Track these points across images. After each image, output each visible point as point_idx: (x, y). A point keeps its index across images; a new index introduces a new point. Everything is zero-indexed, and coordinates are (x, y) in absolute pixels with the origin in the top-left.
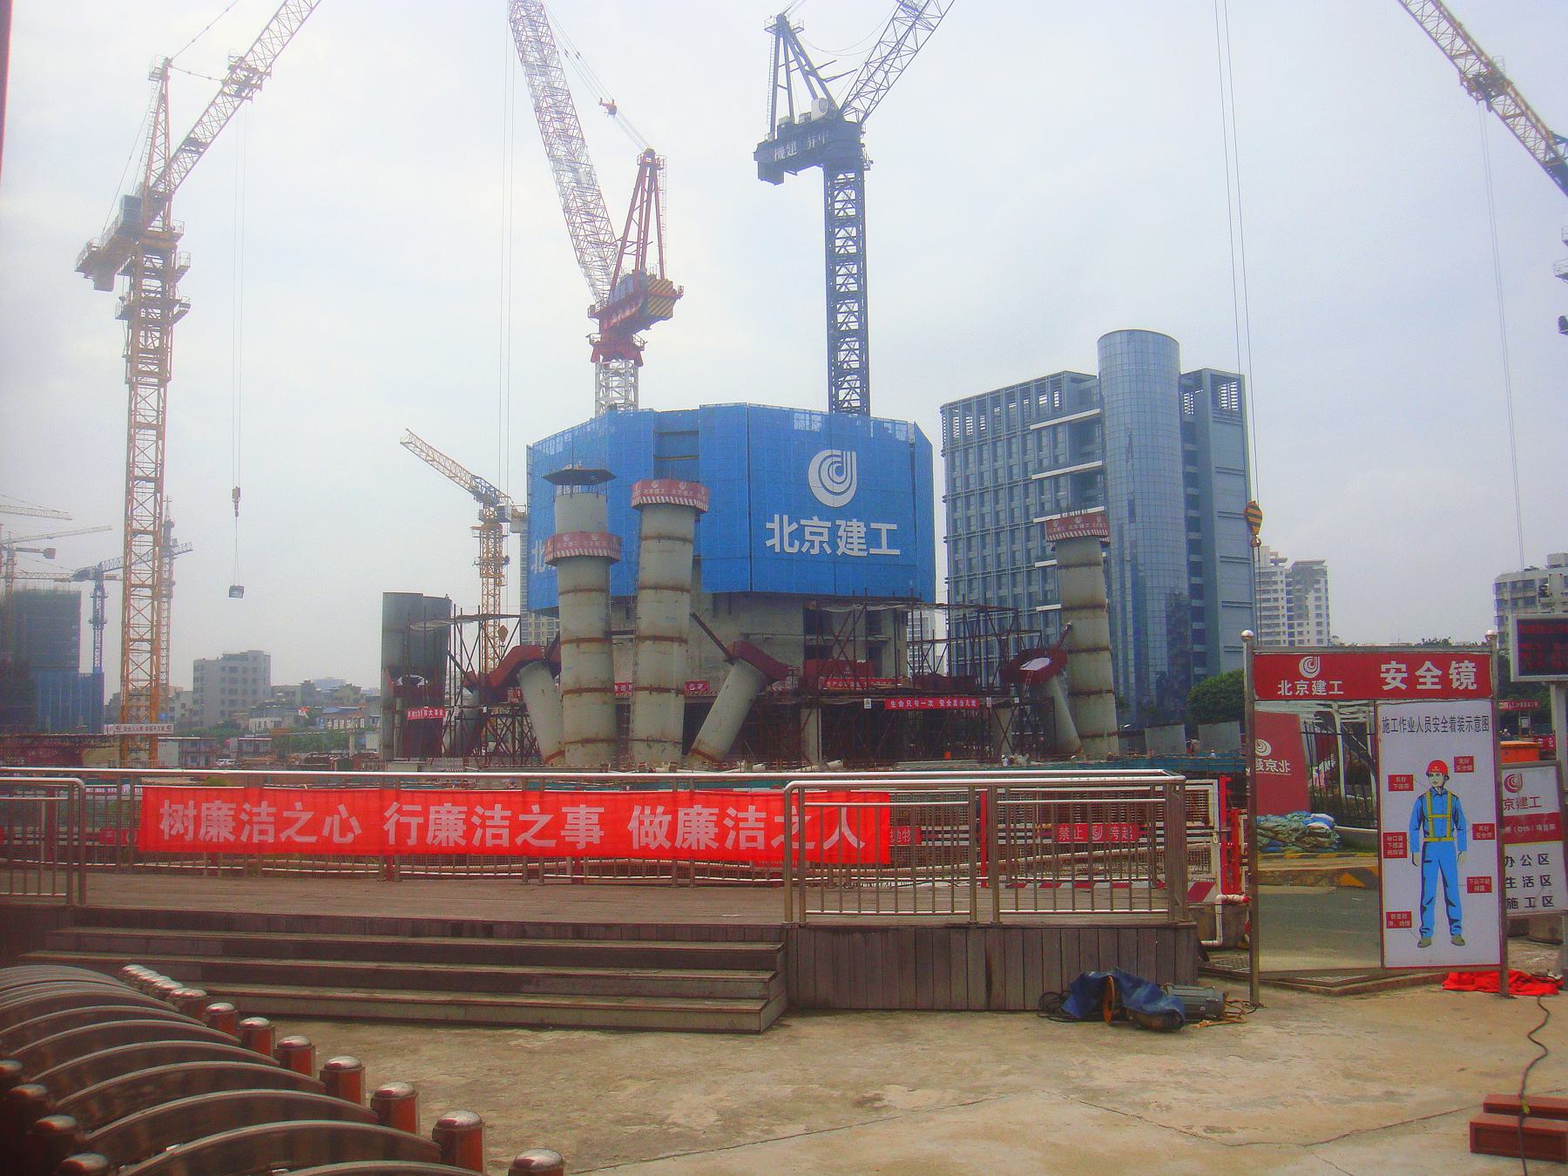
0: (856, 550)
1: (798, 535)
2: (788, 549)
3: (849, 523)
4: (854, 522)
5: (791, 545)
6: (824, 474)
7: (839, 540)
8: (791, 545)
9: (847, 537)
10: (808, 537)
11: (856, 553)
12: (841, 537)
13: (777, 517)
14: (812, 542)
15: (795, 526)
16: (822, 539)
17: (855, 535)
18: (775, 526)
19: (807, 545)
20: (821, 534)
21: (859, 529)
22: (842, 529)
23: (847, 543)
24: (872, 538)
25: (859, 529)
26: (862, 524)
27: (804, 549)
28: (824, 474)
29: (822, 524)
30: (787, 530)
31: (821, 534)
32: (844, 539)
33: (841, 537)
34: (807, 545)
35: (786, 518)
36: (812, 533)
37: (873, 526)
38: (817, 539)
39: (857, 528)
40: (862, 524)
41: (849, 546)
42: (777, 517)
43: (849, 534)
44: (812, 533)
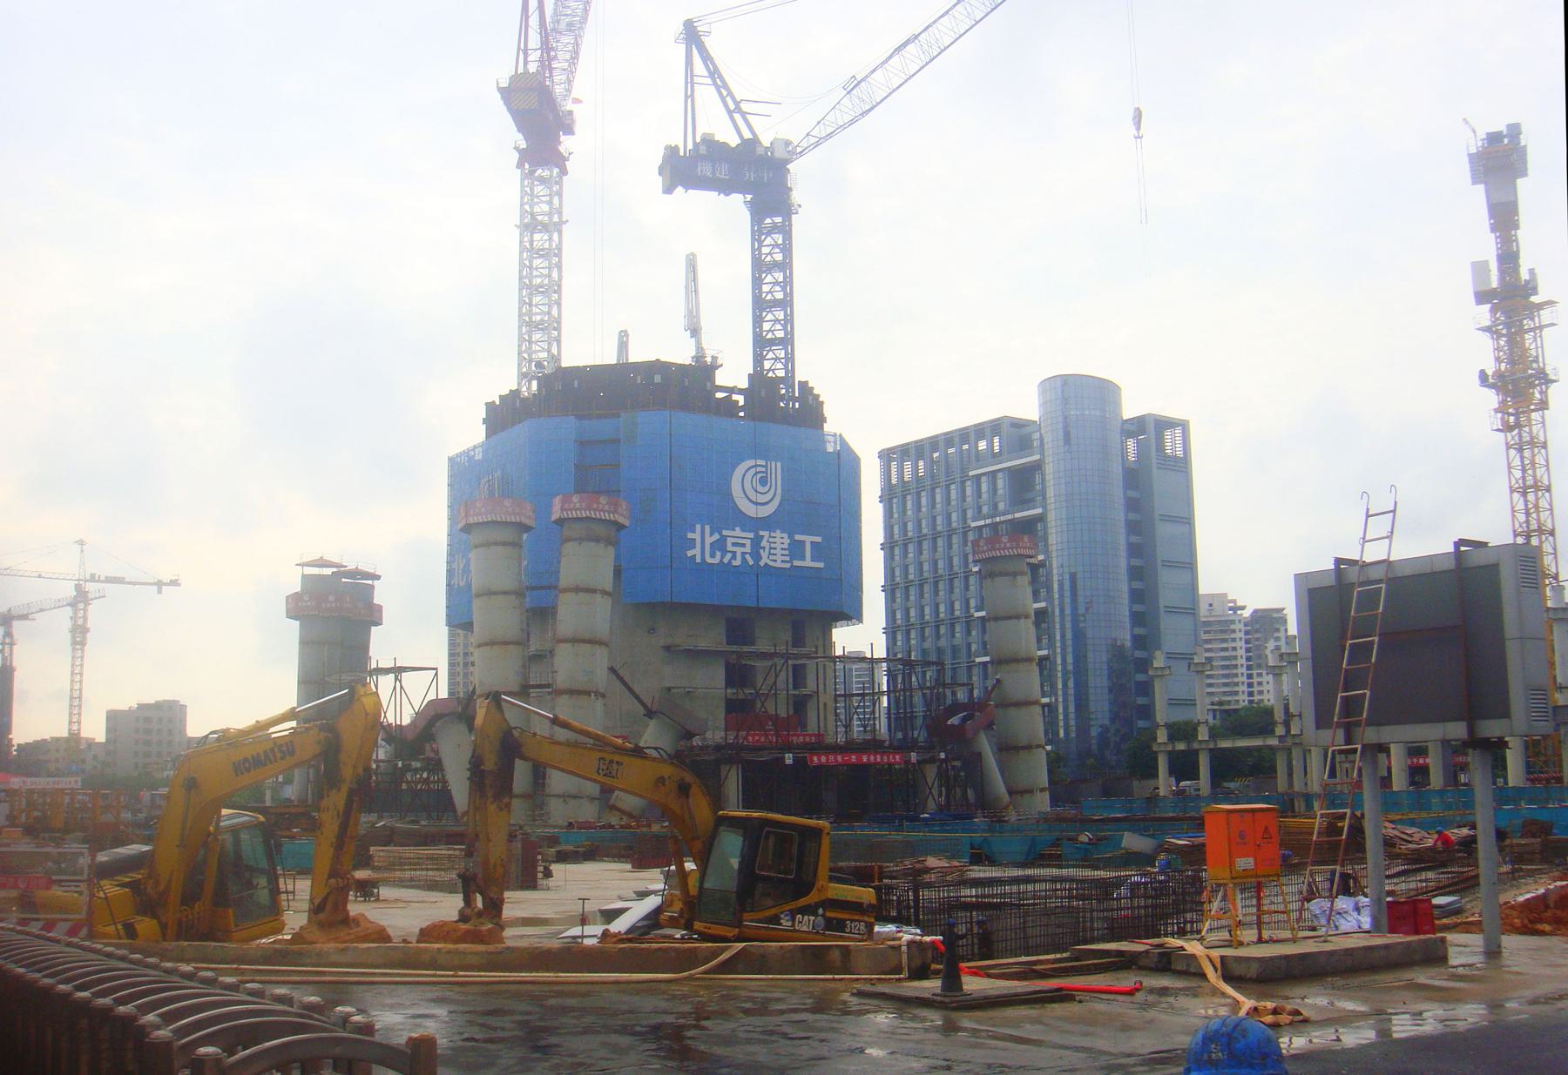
0: (779, 561)
1: (720, 545)
2: (709, 560)
3: (772, 534)
4: (778, 534)
5: (713, 555)
6: (748, 486)
7: (761, 551)
8: (713, 555)
9: (771, 548)
10: (730, 548)
11: (778, 564)
13: (698, 527)
14: (734, 553)
15: (716, 537)
16: (743, 550)
17: (779, 546)
18: (696, 536)
19: (729, 556)
20: (743, 545)
21: (783, 541)
23: (770, 554)
24: (796, 549)
25: (783, 541)
27: (726, 561)
28: (748, 486)
30: (709, 540)
31: (743, 545)
34: (729, 556)
35: (707, 528)
36: (734, 544)
37: (798, 537)
38: (739, 550)
39: (781, 539)
40: (785, 535)
41: (771, 557)
42: (698, 527)
43: (773, 545)
44: (734, 544)
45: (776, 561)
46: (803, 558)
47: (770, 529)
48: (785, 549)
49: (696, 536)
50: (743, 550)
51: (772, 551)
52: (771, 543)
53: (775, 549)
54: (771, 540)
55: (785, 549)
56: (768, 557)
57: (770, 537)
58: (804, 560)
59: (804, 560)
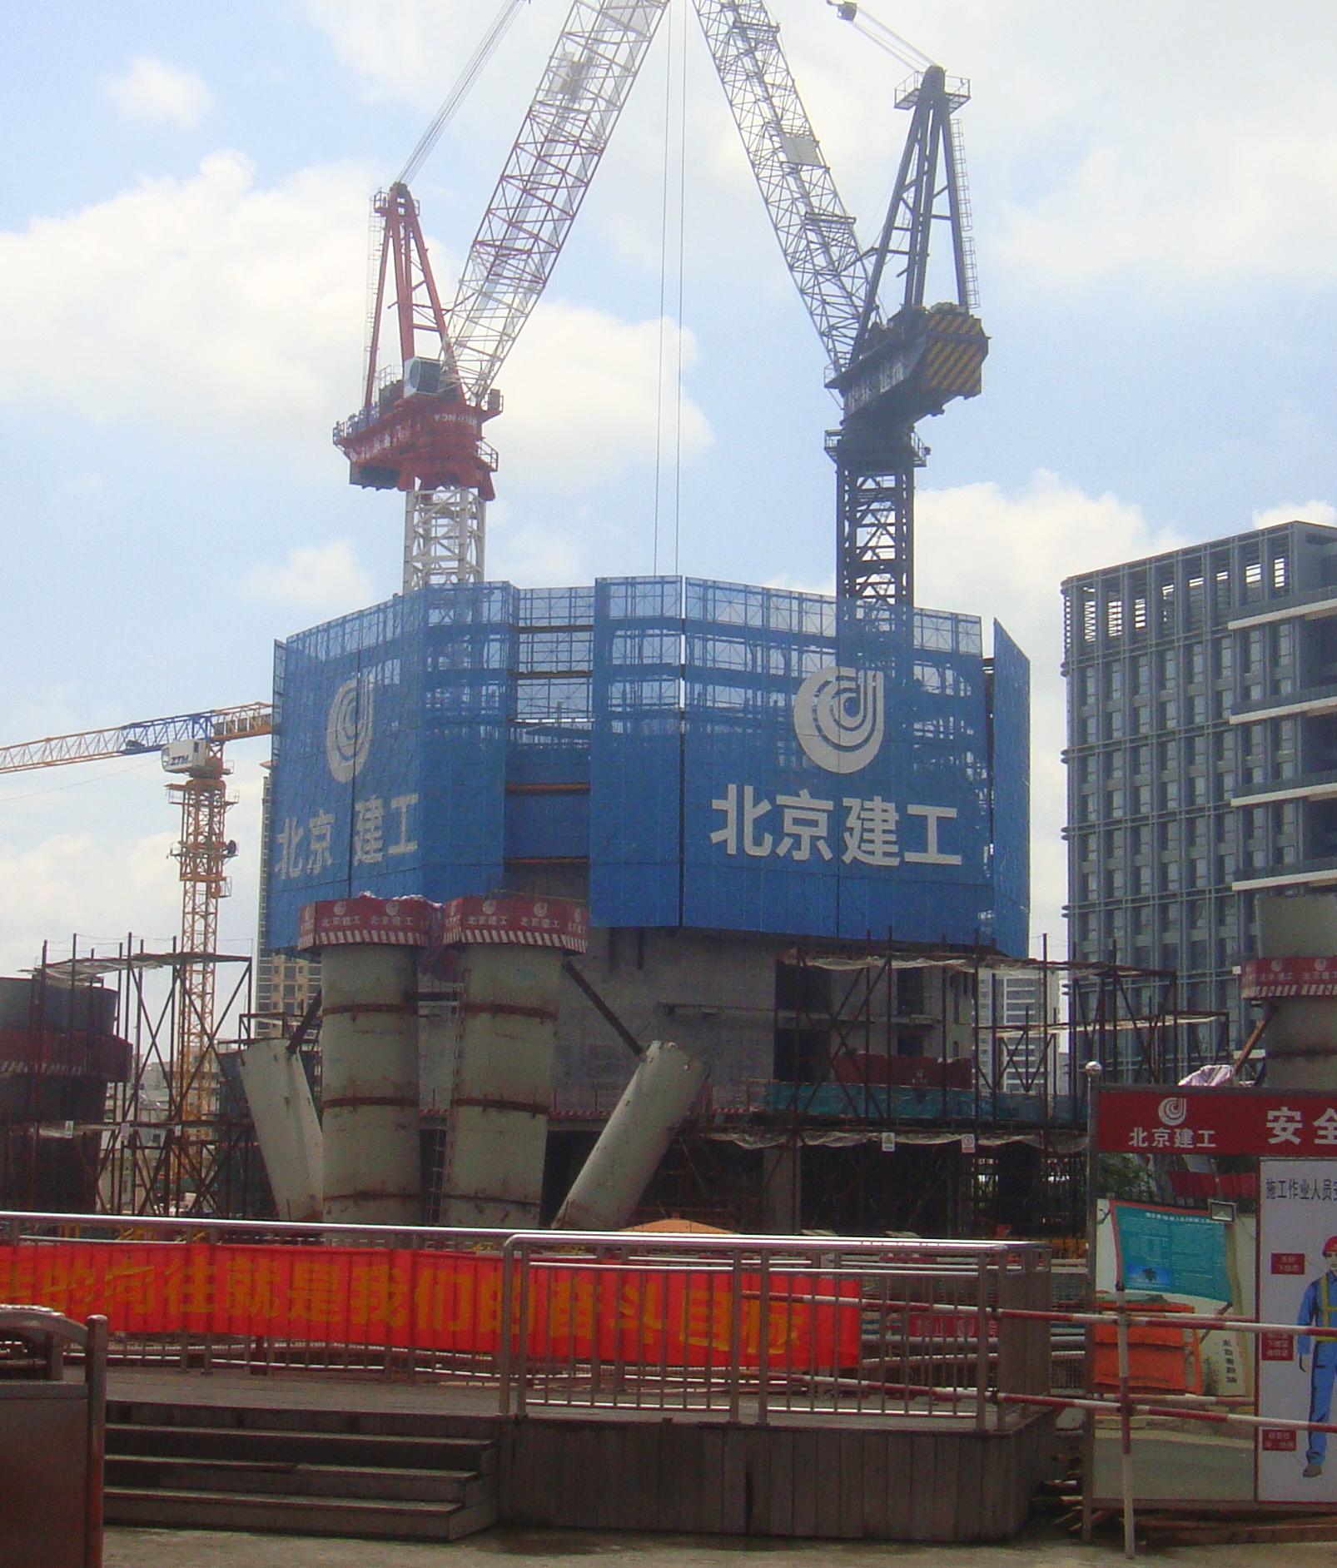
0: (879, 853)
2: (751, 850)
4: (877, 802)
5: (758, 842)
7: (847, 835)
9: (864, 830)
10: (789, 827)
11: (879, 860)
13: (732, 789)
14: (797, 838)
19: (787, 842)
20: (814, 823)
21: (885, 816)
23: (862, 840)
24: (910, 832)
30: (752, 813)
31: (814, 823)
32: (857, 833)
33: (851, 830)
36: (796, 821)
38: (806, 833)
40: (891, 806)
41: (865, 846)
43: (867, 825)
44: (796, 821)
45: (873, 853)
48: (890, 832)
51: (867, 836)
52: (864, 819)
54: (864, 815)
55: (890, 832)
57: (863, 809)
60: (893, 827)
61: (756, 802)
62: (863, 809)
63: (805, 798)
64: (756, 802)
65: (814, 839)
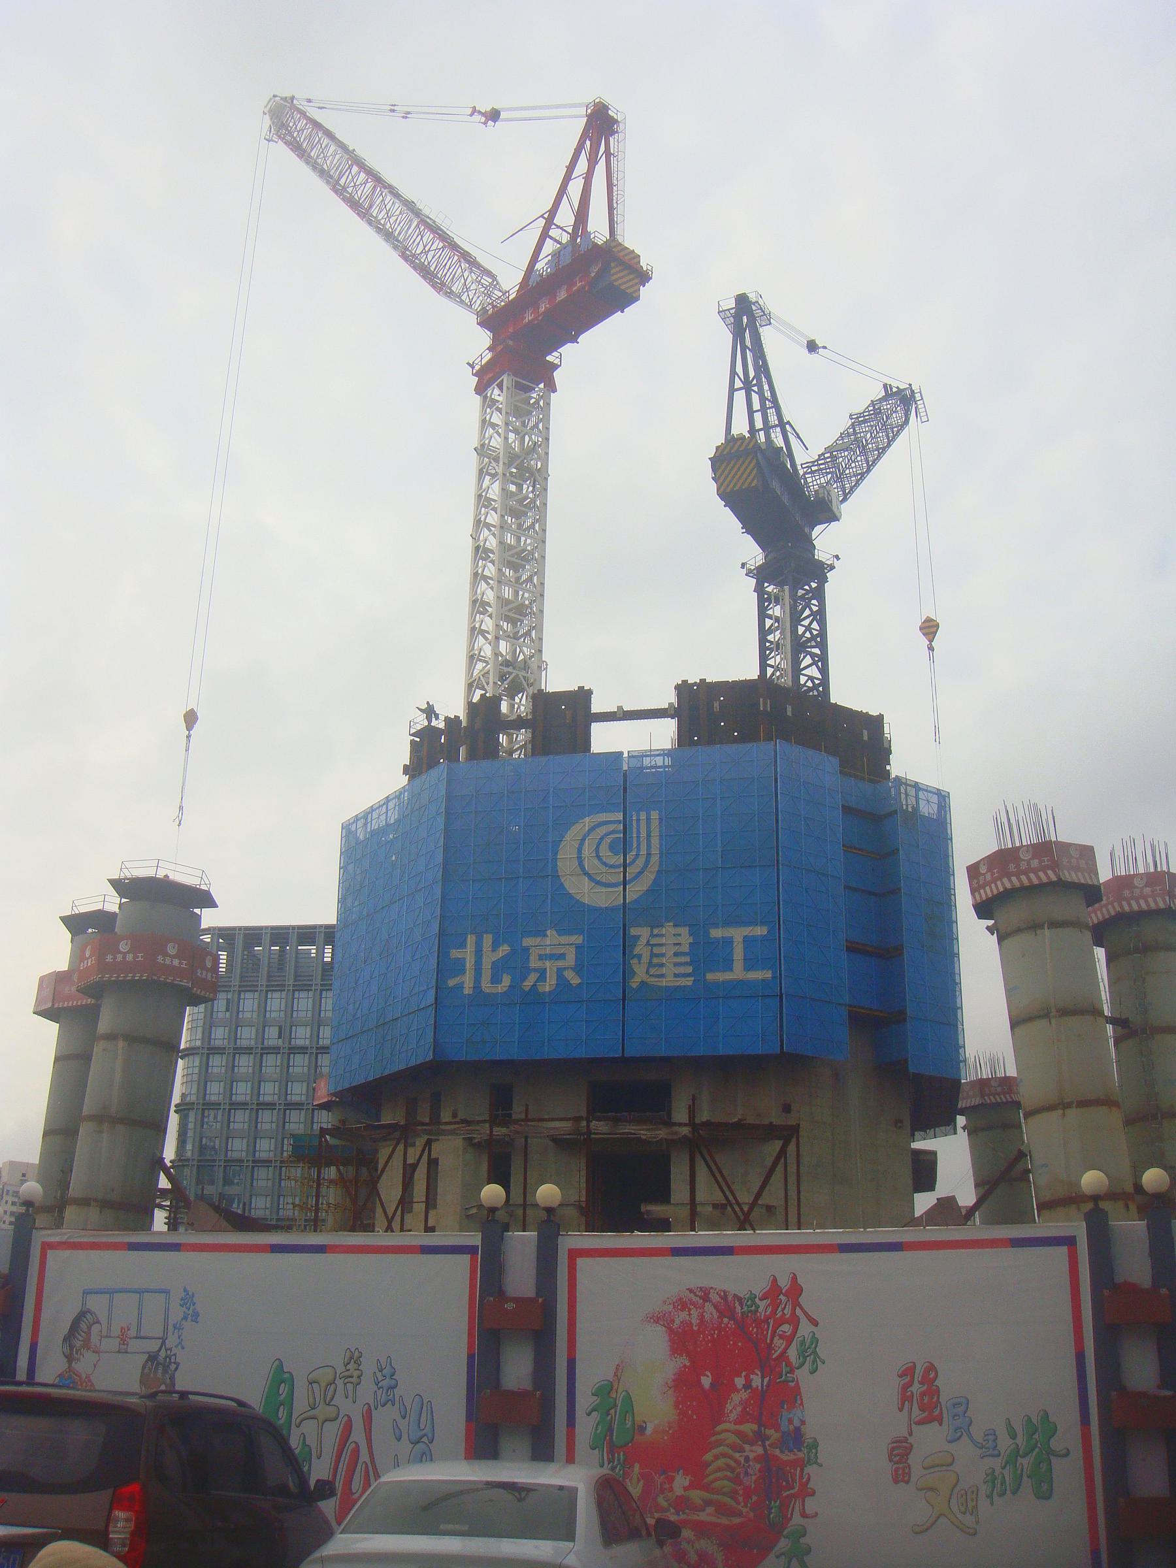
0: (670, 978)
1: (516, 963)
2: (486, 986)
3: (656, 931)
4: (668, 929)
5: (495, 979)
8: (495, 979)
9: (653, 955)
10: (534, 963)
11: (668, 981)
12: (639, 957)
13: (471, 940)
14: (542, 973)
15: (504, 949)
16: (560, 963)
18: (468, 954)
20: (562, 956)
22: (643, 941)
23: (650, 964)
26: (684, 931)
27: (528, 984)
29: (564, 939)
30: (489, 959)
31: (562, 956)
32: (645, 959)
33: (639, 957)
35: (488, 940)
36: (541, 957)
37: (716, 933)
40: (684, 931)
41: (652, 971)
43: (656, 950)
44: (541, 957)
45: (662, 976)
46: (728, 965)
47: (656, 924)
49: (468, 954)
50: (560, 963)
51: (655, 961)
53: (663, 955)
56: (647, 972)
57: (652, 935)
58: (731, 970)
59: (731, 970)
60: (686, 949)
61: (495, 946)
62: (652, 935)
63: (552, 937)
64: (495, 946)
65: (560, 971)
